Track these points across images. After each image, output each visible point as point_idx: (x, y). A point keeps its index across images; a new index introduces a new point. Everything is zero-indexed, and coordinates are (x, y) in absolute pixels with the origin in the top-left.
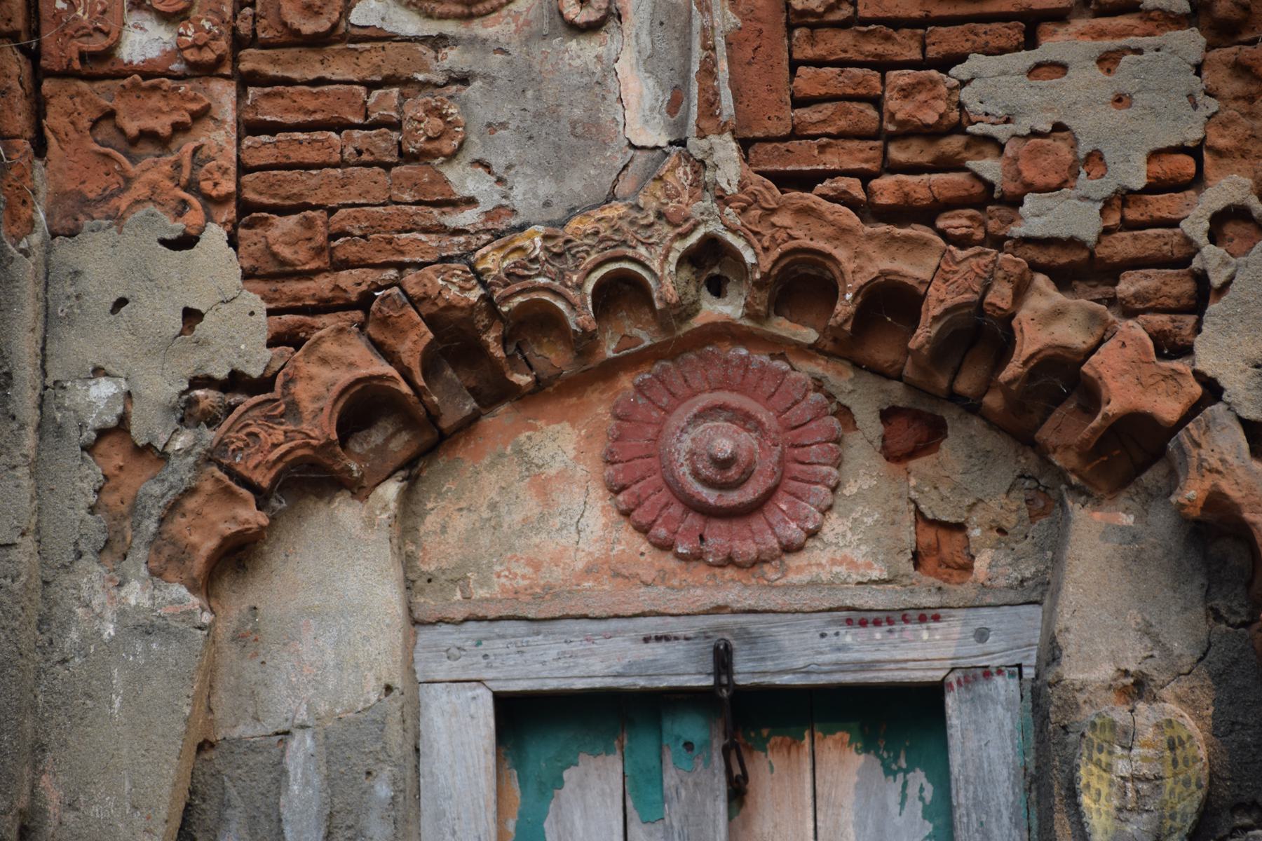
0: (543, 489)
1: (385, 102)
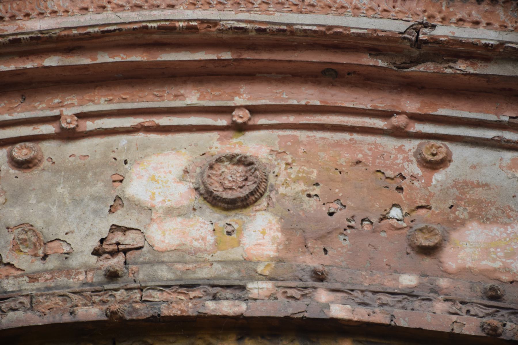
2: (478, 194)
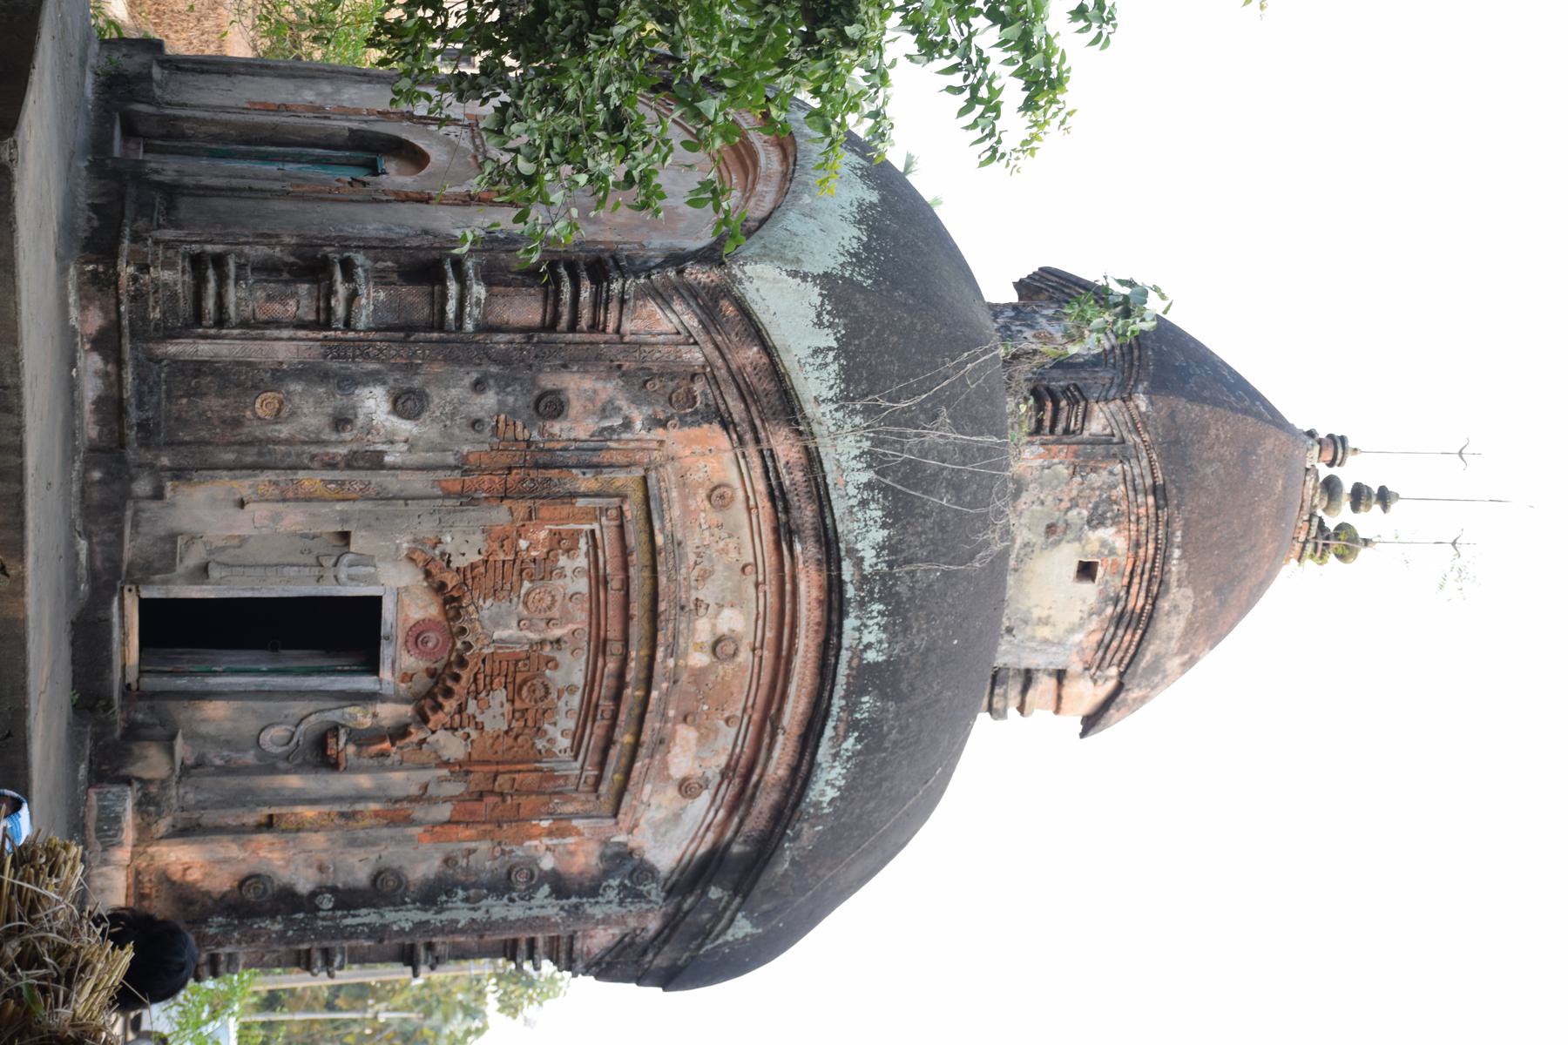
0: (425, 607)
1: (508, 586)
2: (712, 736)
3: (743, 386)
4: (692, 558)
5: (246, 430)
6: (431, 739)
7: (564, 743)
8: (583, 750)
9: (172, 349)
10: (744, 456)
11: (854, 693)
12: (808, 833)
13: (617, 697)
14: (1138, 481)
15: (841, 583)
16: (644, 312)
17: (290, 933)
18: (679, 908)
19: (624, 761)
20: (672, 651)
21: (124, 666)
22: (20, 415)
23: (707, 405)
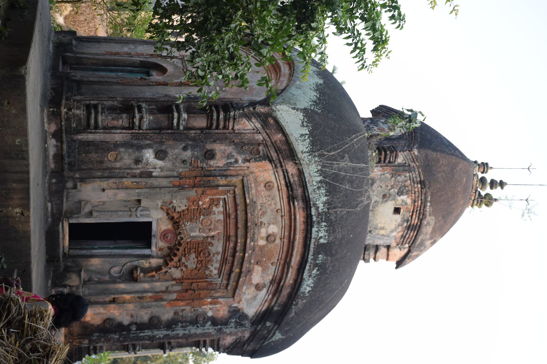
1: (195, 218)
2: (267, 269)
3: (276, 147)
4: (259, 207)
5: (105, 165)
6: (169, 271)
7: (215, 272)
8: (222, 274)
9: (79, 137)
10: (277, 172)
11: (316, 254)
12: (301, 303)
13: (234, 256)
14: (415, 179)
15: (311, 216)
16: (242, 122)
17: (121, 339)
18: (256, 329)
19: (236, 278)
20: (253, 240)
21: (64, 247)
22: (28, 161)
23: (264, 154)
